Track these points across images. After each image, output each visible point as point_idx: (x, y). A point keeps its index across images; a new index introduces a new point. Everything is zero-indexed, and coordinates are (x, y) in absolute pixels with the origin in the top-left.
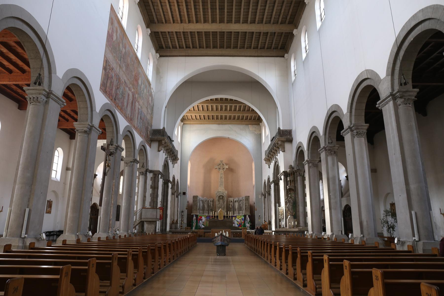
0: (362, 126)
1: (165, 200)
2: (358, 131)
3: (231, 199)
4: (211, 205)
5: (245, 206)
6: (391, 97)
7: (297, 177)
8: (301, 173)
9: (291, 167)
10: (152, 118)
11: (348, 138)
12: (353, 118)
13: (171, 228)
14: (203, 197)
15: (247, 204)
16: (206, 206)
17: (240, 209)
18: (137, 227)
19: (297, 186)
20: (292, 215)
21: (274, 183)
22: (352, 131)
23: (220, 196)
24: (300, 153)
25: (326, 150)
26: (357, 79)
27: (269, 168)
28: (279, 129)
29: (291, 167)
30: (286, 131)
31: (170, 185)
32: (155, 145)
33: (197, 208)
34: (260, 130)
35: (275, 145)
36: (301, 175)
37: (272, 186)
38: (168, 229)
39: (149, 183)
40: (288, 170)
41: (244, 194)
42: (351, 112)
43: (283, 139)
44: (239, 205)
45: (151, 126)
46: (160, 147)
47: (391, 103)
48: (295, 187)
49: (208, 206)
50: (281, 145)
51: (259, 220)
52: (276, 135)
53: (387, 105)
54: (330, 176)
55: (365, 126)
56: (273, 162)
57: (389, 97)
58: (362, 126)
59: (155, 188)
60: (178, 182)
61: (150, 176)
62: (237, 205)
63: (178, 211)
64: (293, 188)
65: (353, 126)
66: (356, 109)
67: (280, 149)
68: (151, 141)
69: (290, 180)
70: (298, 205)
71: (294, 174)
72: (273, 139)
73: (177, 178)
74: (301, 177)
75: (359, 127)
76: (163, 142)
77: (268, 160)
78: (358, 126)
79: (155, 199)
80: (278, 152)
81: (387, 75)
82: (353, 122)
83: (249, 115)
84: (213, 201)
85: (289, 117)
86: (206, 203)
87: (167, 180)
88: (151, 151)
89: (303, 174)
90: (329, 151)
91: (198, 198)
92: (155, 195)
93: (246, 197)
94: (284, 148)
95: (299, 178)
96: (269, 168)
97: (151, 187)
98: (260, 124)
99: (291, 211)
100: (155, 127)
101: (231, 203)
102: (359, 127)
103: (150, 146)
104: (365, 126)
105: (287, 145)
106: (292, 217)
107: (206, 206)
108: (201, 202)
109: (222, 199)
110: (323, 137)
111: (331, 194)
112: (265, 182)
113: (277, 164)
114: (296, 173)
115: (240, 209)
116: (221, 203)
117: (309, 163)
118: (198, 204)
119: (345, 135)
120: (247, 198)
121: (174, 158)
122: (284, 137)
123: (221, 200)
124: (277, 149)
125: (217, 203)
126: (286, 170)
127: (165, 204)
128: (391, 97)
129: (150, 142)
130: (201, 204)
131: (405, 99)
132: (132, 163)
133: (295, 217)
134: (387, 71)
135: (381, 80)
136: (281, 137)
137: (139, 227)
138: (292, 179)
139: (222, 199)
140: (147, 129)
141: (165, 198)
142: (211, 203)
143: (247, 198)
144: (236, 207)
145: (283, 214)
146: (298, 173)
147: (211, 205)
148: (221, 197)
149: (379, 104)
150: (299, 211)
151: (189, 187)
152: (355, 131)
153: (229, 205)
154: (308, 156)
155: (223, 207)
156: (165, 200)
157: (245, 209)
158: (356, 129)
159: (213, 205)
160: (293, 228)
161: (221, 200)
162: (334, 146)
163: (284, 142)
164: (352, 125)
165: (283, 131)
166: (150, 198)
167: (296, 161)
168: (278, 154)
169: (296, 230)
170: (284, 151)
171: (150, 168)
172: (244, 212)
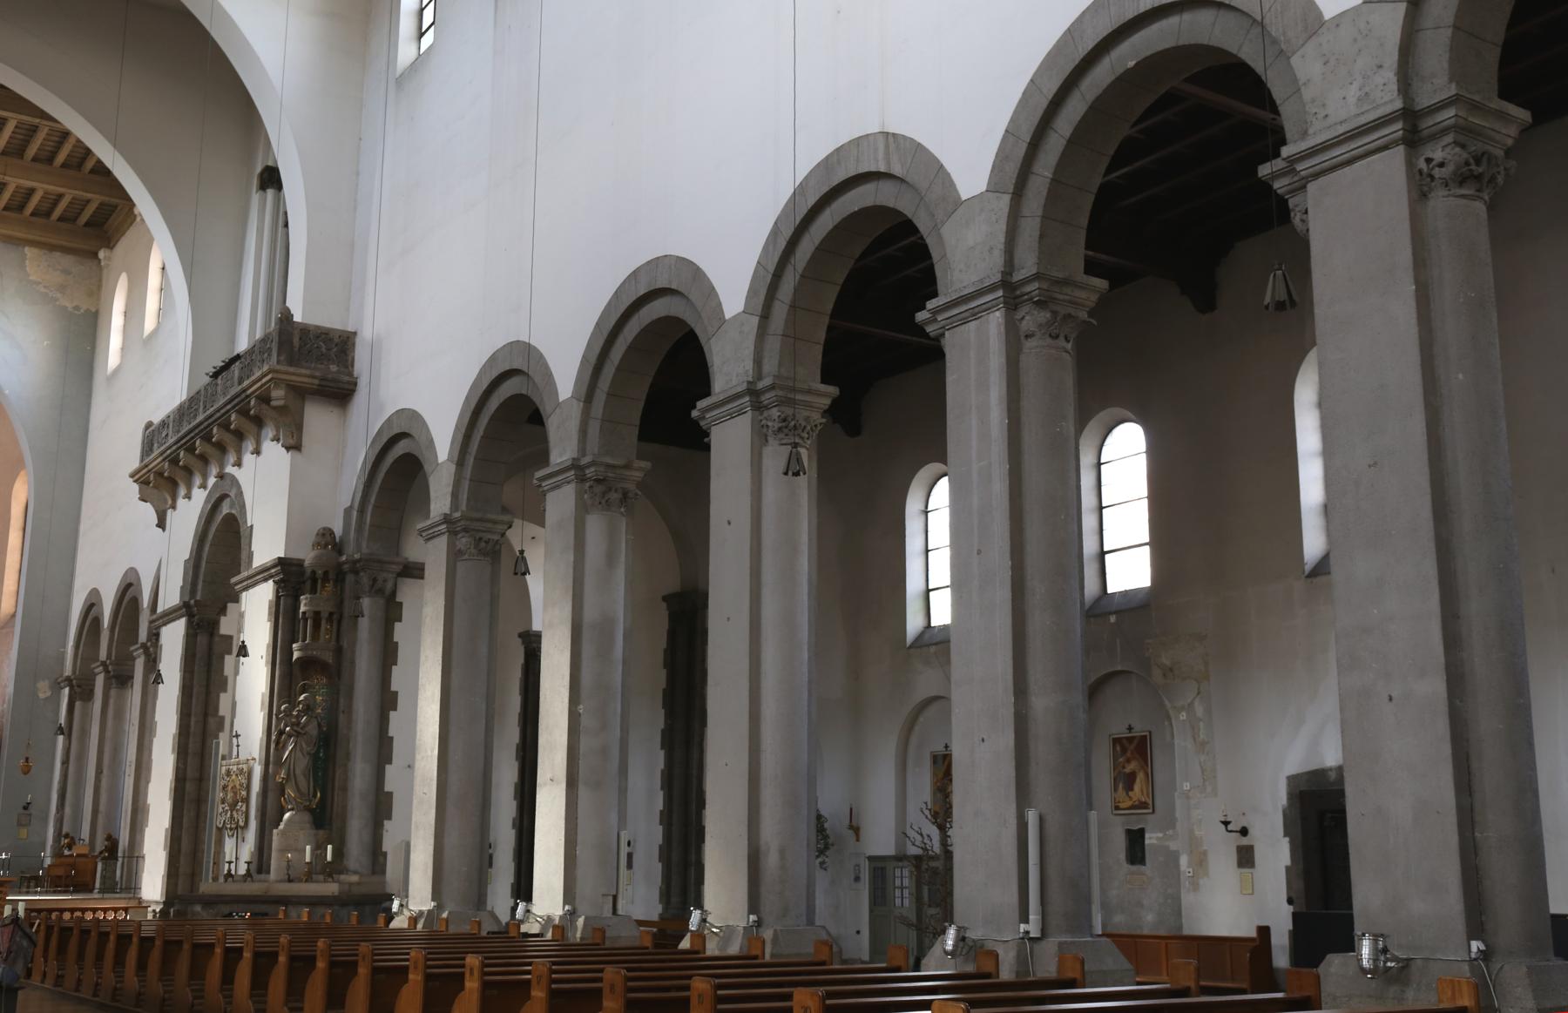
0: (809, 392)
2: (789, 411)
6: (1000, 293)
9: (326, 537)
11: (730, 441)
12: (773, 344)
19: (353, 644)
21: (190, 616)
22: (758, 407)
24: (397, 467)
25: (581, 479)
26: (826, 164)
27: (161, 524)
28: (286, 316)
29: (326, 537)
30: (324, 335)
34: (98, 292)
35: (240, 404)
36: (380, 591)
37: (173, 637)
40: (307, 555)
42: (765, 316)
43: (302, 375)
47: (997, 318)
48: (339, 651)
50: (282, 410)
51: (24, 832)
52: (259, 349)
53: (973, 325)
54: (590, 614)
55: (824, 395)
56: (200, 496)
57: (992, 289)
58: (809, 392)
64: (328, 657)
65: (772, 387)
66: (793, 307)
67: (269, 432)
69: (317, 616)
70: (348, 756)
71: (340, 577)
72: (227, 366)
74: (381, 601)
75: (799, 397)
77: (161, 479)
78: (794, 390)
80: (249, 445)
81: (994, 187)
82: (770, 366)
83: (42, 188)
85: (344, 258)
89: (389, 585)
90: (599, 489)
94: (298, 428)
96: (161, 524)
99: (301, 779)
102: (799, 397)
104: (824, 395)
105: (317, 418)
106: (307, 817)
110: (576, 410)
111: (581, 708)
112: (92, 606)
113: (225, 509)
114: (350, 578)
117: (452, 533)
119: (719, 420)
122: (305, 370)
124: (247, 426)
126: (297, 554)
128: (1000, 293)
131: (1054, 313)
133: (324, 817)
134: (997, 168)
135: (958, 203)
136: (291, 362)
138: (326, 608)
145: (247, 800)
146: (365, 579)
149: (936, 311)
150: (345, 789)
152: (775, 413)
154: (455, 495)
158: (781, 402)
160: (309, 878)
162: (627, 466)
163: (301, 393)
164: (767, 382)
165: (305, 330)
167: (362, 511)
168: (248, 458)
169: (330, 888)
170: (294, 447)
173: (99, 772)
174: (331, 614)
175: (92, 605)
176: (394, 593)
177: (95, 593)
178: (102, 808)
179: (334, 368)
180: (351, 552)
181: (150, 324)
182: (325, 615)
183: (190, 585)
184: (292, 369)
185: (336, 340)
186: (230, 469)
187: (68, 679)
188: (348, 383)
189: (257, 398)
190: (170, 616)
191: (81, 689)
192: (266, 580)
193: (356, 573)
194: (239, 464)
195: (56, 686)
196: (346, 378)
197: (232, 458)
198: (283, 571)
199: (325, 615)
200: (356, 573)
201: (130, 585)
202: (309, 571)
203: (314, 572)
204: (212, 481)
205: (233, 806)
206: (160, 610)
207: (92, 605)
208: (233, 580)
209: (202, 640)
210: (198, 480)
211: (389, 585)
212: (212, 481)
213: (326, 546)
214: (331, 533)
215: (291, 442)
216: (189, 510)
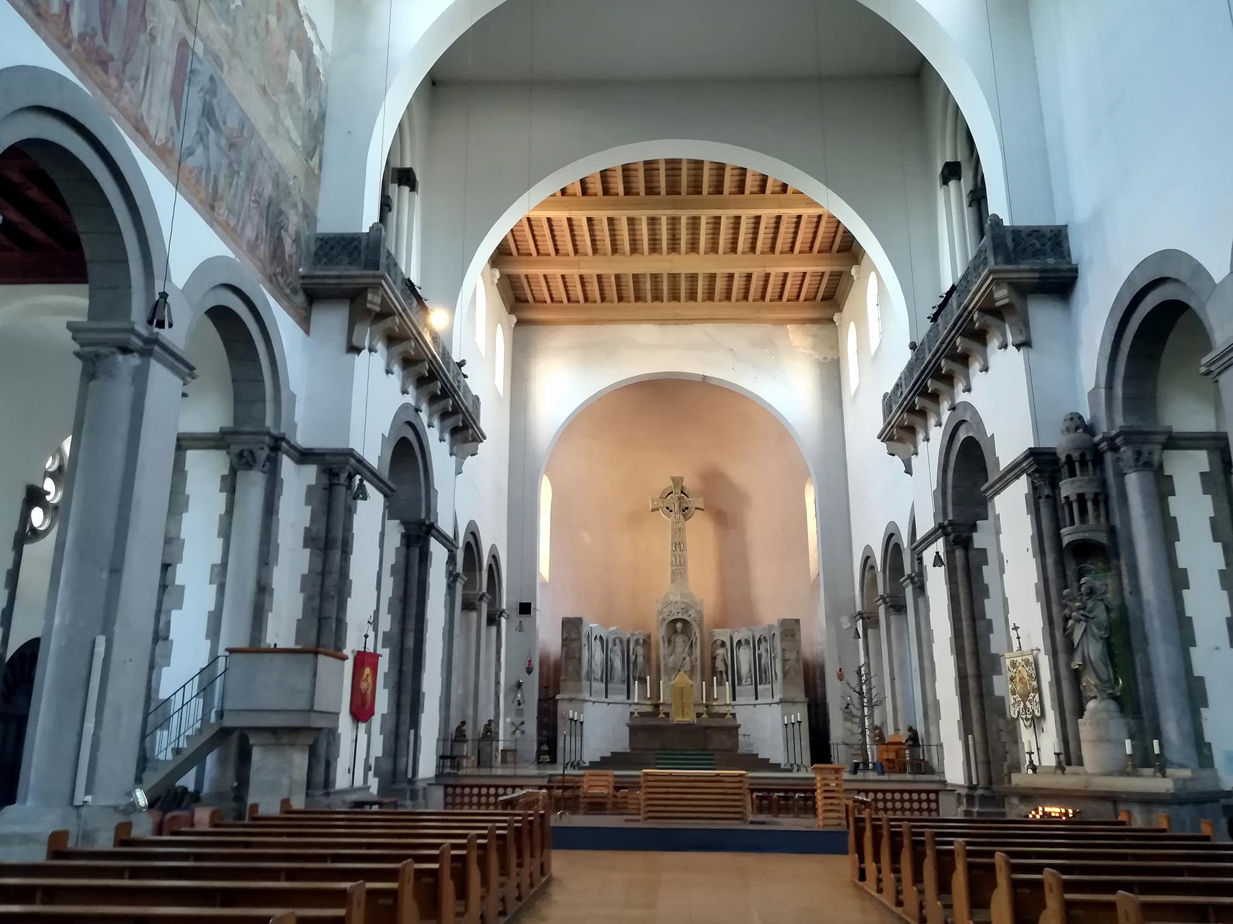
1: (411, 624)
3: (722, 635)
4: (640, 659)
5: (784, 661)
7: (1121, 476)
8: (1146, 449)
10: (314, 177)
13: (448, 758)
14: (605, 624)
15: (791, 656)
16: (618, 664)
17: (760, 675)
18: (210, 760)
20: (1113, 697)
21: (946, 535)
23: (675, 621)
27: (909, 471)
29: (1076, 423)
31: (438, 552)
32: (332, 320)
33: (578, 673)
36: (1148, 465)
38: (427, 766)
39: (294, 514)
40: (1058, 441)
41: (770, 613)
43: (1026, 269)
44: (756, 659)
45: (309, 216)
46: (358, 328)
48: (1112, 531)
49: (627, 662)
56: (937, 435)
59: (330, 543)
60: (495, 558)
61: (297, 480)
62: (744, 658)
63: (498, 683)
64: (1103, 538)
68: (311, 297)
69: (1081, 498)
70: (1145, 639)
73: (493, 537)
74: (1150, 475)
76: (374, 301)
79: (331, 610)
80: (975, 366)
84: (647, 642)
86: (618, 648)
87: (422, 523)
88: (299, 348)
91: (585, 631)
92: (332, 580)
93: (784, 622)
94: (1026, 324)
95: (1133, 481)
96: (909, 471)
97: (310, 540)
98: (835, 318)
100: (330, 222)
101: (720, 651)
103: (305, 323)
105: (1042, 314)
106: (1112, 705)
107: (618, 664)
108: (597, 646)
109: (683, 632)
112: (867, 559)
114: (1109, 457)
115: (760, 675)
116: (679, 650)
118: (585, 654)
120: (790, 629)
121: (458, 420)
123: (679, 640)
125: (663, 650)
126: (1049, 442)
127: (410, 643)
129: (300, 299)
130: (598, 656)
132: (135, 360)
133: (1135, 707)
136: (1008, 262)
137: (222, 761)
138: (1089, 491)
139: (683, 632)
140: (274, 220)
141: (413, 610)
142: (640, 650)
143: (790, 629)
144: (745, 669)
145: (1039, 690)
146: (1127, 452)
147: (640, 659)
148: (679, 625)
150: (1149, 675)
151: (544, 584)
153: (714, 658)
155: (687, 667)
156: (411, 624)
157: (785, 674)
159: (647, 659)
161: (679, 640)
163: (1023, 290)
165: (1016, 232)
166: (300, 598)
171: (303, 439)
172: (778, 686)
173: (893, 679)
174: (1096, 495)
175: (868, 558)
176: (1161, 466)
177: (868, 548)
178: (899, 705)
179: (1051, 261)
180: (1103, 428)
181: (874, 343)
182: (1089, 497)
183: (942, 509)
184: (1010, 267)
185: (1049, 235)
186: (961, 397)
187: (860, 613)
188: (1070, 270)
189: (980, 310)
190: (929, 539)
191: (870, 620)
192: (1017, 477)
193: (1115, 449)
194: (968, 389)
195: (854, 618)
196: (1068, 266)
197: (960, 387)
198: (1037, 462)
199: (1089, 497)
200: (1115, 449)
201: (892, 535)
202: (1063, 458)
203: (1069, 457)
204: (946, 415)
205: (1025, 697)
206: (919, 537)
207: (868, 558)
208: (983, 488)
209: (959, 553)
210: (932, 421)
211: (1156, 458)
212: (946, 415)
213: (1077, 428)
214: (1080, 417)
215: (1021, 339)
216: (931, 447)
